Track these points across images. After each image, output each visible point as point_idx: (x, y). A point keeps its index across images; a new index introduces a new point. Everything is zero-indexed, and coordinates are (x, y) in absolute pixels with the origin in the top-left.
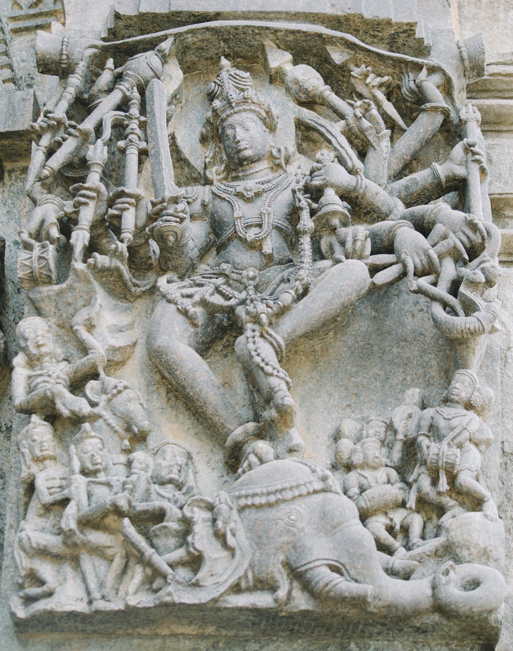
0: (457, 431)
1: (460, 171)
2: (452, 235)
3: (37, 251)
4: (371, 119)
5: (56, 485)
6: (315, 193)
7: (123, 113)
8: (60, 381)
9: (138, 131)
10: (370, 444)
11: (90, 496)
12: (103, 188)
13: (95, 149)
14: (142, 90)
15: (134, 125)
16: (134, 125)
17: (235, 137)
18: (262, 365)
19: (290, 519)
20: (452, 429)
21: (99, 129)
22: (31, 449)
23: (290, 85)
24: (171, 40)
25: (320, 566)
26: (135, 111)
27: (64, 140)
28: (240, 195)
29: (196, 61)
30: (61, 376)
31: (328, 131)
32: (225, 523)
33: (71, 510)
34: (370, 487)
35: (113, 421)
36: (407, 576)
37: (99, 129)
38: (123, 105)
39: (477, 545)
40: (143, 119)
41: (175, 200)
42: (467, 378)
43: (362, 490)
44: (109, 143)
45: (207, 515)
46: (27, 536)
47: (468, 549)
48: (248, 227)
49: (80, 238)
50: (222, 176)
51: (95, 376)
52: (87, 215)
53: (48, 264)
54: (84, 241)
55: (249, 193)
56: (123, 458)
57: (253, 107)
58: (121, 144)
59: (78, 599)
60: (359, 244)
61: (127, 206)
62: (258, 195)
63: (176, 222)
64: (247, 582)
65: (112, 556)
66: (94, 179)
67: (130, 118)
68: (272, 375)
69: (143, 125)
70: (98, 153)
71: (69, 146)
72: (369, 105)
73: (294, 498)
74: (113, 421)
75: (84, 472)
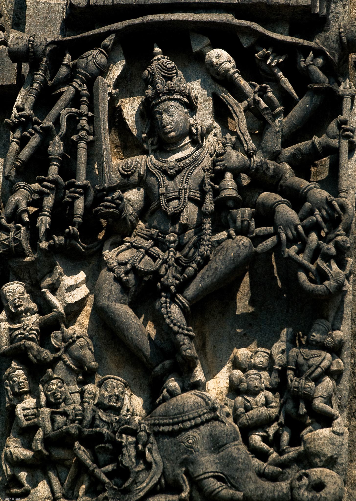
0: (312, 369)
1: (334, 142)
2: (317, 212)
3: (12, 235)
4: (268, 101)
5: (30, 414)
6: (218, 177)
7: (74, 110)
8: (33, 332)
9: (87, 127)
10: (252, 376)
11: (53, 421)
12: (61, 180)
13: (54, 144)
14: (90, 88)
15: (83, 122)
16: (83, 122)
17: (162, 123)
18: (171, 325)
19: (189, 443)
20: (310, 367)
21: (57, 122)
22: (12, 387)
23: (208, 67)
24: (112, 37)
25: (208, 478)
26: (84, 108)
27: (32, 135)
28: (164, 172)
29: (136, 47)
30: (33, 327)
31: (234, 111)
32: (144, 445)
33: (39, 435)
34: (252, 409)
35: (69, 362)
36: (273, 478)
37: (57, 122)
38: (75, 101)
39: (324, 455)
40: (90, 114)
41: (112, 190)
42: (321, 327)
43: (247, 409)
44: (65, 139)
45: (131, 439)
46: (10, 452)
47: (320, 458)
48: (169, 201)
49: (44, 222)
50: (155, 147)
51: (58, 328)
52: (49, 201)
53: (21, 244)
54: (46, 226)
55: (171, 171)
56: (78, 389)
57: (175, 96)
58: (74, 137)
59: (45, 498)
60: (246, 223)
61: (77, 195)
62: (179, 172)
63: (113, 207)
64: (161, 486)
65: (69, 465)
66: (54, 170)
67: (81, 115)
68: (178, 333)
69: (91, 121)
70: (56, 147)
71: (34, 140)
72: (266, 88)
73: (192, 427)
74: (69, 362)
75: (49, 404)
